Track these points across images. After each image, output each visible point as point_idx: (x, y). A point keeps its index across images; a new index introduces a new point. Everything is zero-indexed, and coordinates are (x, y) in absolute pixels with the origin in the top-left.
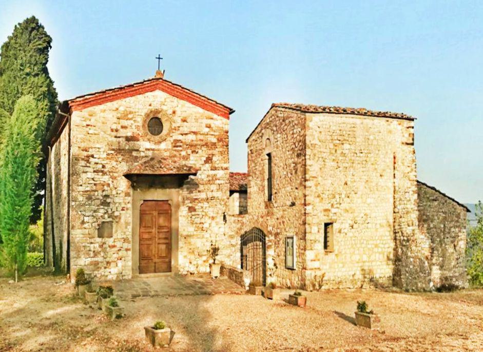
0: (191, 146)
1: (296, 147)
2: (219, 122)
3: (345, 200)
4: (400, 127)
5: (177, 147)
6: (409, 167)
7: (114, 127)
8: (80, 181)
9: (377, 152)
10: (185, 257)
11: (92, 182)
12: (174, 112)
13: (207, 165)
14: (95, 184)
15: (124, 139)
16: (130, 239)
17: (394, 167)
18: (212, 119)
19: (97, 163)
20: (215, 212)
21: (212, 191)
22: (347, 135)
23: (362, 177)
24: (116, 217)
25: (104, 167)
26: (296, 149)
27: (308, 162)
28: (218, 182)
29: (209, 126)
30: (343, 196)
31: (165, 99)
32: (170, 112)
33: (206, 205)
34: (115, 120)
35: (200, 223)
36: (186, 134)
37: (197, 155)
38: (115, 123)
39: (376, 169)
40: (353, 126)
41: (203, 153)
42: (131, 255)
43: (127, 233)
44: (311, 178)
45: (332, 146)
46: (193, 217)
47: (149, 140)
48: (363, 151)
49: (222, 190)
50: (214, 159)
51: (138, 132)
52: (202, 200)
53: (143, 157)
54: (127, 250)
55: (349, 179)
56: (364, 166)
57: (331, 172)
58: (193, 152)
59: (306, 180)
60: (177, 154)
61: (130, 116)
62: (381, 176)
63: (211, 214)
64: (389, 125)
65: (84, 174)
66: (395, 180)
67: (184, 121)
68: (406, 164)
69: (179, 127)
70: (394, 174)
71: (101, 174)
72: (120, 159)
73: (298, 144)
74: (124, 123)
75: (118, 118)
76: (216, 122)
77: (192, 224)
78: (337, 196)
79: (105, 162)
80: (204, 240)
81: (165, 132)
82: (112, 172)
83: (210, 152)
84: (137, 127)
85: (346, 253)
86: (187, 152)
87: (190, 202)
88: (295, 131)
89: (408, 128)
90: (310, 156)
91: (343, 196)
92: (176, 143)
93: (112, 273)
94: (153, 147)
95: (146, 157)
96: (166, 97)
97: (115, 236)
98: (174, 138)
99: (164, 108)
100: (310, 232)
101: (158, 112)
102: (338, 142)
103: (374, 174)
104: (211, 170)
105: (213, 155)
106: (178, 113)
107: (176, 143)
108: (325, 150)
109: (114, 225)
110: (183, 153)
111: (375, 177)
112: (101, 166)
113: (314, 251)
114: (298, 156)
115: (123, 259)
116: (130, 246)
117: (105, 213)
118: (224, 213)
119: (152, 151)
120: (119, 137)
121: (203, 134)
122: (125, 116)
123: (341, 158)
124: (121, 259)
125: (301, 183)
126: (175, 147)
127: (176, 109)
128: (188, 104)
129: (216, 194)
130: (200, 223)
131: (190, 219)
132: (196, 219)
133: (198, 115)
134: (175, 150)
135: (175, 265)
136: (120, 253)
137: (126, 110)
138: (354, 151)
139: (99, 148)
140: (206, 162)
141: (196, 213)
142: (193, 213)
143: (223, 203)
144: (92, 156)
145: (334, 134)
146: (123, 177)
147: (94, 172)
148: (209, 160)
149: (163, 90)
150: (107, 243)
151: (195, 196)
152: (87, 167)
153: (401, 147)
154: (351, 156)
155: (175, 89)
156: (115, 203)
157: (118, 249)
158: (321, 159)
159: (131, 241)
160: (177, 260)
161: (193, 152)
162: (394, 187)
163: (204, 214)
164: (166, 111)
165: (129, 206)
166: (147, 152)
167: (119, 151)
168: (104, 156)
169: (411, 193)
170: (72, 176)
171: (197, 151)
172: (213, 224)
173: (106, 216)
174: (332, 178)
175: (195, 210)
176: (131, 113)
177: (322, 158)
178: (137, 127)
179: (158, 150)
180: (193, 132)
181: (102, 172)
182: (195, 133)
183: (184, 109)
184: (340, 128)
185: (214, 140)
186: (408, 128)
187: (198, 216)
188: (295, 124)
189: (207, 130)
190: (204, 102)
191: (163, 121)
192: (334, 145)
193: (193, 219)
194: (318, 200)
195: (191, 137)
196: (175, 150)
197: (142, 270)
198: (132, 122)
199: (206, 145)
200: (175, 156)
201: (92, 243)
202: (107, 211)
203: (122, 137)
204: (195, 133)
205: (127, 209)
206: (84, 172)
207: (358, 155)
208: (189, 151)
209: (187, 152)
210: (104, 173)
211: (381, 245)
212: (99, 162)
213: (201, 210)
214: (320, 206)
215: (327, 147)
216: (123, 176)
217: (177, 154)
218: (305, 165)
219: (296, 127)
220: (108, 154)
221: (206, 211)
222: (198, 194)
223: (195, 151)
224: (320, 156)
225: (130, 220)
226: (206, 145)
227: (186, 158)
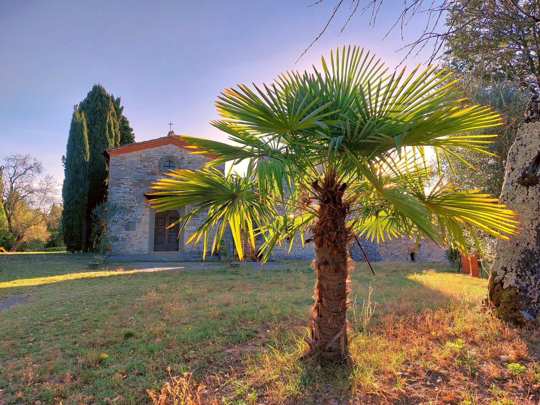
7: (139, 166)
11: (123, 199)
14: (124, 200)
15: (145, 174)
19: (126, 188)
24: (138, 219)
25: (130, 190)
31: (176, 150)
43: (146, 228)
54: (145, 238)
71: (128, 194)
82: (136, 193)
97: (137, 230)
99: (175, 155)
109: (137, 224)
116: (147, 236)
117: (131, 217)
136: (141, 240)
144: (123, 184)
149: (174, 144)
156: (138, 211)
164: (177, 157)
165: (148, 213)
167: (141, 181)
168: (131, 183)
173: (131, 218)
198: (151, 163)
201: (121, 233)
202: (132, 216)
205: (146, 215)
206: (116, 193)
210: (131, 194)
220: (134, 183)
225: (148, 221)
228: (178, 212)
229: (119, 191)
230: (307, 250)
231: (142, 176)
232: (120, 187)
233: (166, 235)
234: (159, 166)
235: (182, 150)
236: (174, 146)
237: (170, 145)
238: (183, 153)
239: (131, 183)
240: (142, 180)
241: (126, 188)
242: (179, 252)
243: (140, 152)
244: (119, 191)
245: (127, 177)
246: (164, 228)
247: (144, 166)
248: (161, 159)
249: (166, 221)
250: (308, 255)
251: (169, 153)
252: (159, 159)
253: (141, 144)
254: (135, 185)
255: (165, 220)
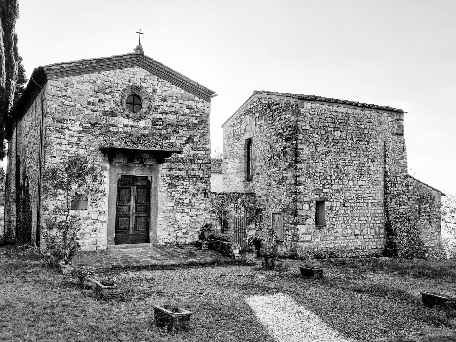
0: (172, 126)
1: (284, 132)
2: (200, 104)
3: (336, 181)
4: (390, 119)
5: (157, 125)
6: (399, 154)
7: (91, 100)
8: (54, 153)
9: (368, 140)
10: (164, 229)
11: (67, 154)
12: (154, 91)
13: (188, 145)
15: (101, 114)
16: (107, 212)
17: (385, 154)
18: (193, 100)
19: (72, 136)
20: (195, 189)
21: (193, 170)
22: (338, 123)
23: (354, 162)
25: (79, 140)
26: (285, 134)
27: (300, 146)
28: (199, 161)
29: (190, 107)
30: (334, 178)
31: (145, 76)
32: (150, 90)
33: (186, 182)
34: (93, 93)
35: (180, 199)
36: (167, 114)
37: (178, 135)
38: (92, 96)
39: (366, 155)
40: (344, 114)
41: (185, 133)
42: (106, 227)
43: (103, 206)
44: (302, 161)
45: (323, 133)
46: (174, 193)
47: (127, 116)
48: (354, 139)
49: (203, 170)
50: (196, 139)
51: (116, 107)
52: (182, 177)
53: (121, 133)
54: (102, 222)
55: (341, 163)
56: (355, 152)
57: (322, 156)
58: (173, 131)
59: (297, 162)
60: (157, 132)
61: (108, 90)
62: (372, 161)
63: (192, 191)
64: (380, 116)
65: (58, 146)
66: (386, 166)
67: (164, 100)
68: (396, 152)
69: (159, 106)
70: (385, 161)
71: (76, 147)
72: (97, 133)
73: (287, 129)
74: (102, 97)
75: (96, 92)
76: (197, 104)
77: (173, 199)
78: (329, 178)
79: (81, 135)
80: (184, 214)
81: (144, 110)
82: (88, 146)
83: (192, 133)
84: (115, 102)
85: (337, 228)
86: (167, 131)
87: (170, 179)
88: (283, 117)
89: (398, 120)
90: (301, 140)
91: (334, 178)
92: (156, 122)
93: (85, 244)
94: (132, 123)
95: (124, 133)
96: (146, 74)
98: (154, 116)
99: (144, 85)
100: (302, 209)
101: (138, 89)
102: (330, 129)
103: (365, 160)
104: (193, 150)
105: (195, 136)
106: (159, 91)
107: (156, 122)
108: (316, 136)
110: (163, 132)
111: (366, 163)
112: (76, 139)
113: (306, 226)
114: (287, 140)
115: (98, 230)
116: (106, 218)
118: (205, 190)
119: (130, 128)
120: (96, 111)
121: (184, 115)
122: (103, 90)
123: (332, 144)
124: (95, 231)
125: (290, 165)
126: (154, 125)
127: (157, 88)
128: (169, 84)
129: (196, 173)
130: (180, 199)
131: (169, 194)
132: (176, 195)
133: (179, 96)
134: (155, 129)
135: (153, 237)
136: (95, 226)
137: (104, 84)
138: (345, 137)
139: (74, 120)
140: (187, 142)
141: (177, 189)
142: (173, 189)
143: (204, 181)
144: (68, 128)
145: (325, 121)
146: (100, 152)
147: (69, 144)
148: (190, 140)
149: (143, 67)
150: (81, 215)
151: (176, 173)
152: (62, 139)
153: (391, 136)
154: (342, 142)
155: (156, 68)
157: (93, 221)
158: (312, 143)
159: (107, 214)
160: (155, 233)
161: (173, 131)
162: (386, 172)
163: (184, 190)
166: (126, 128)
168: (81, 128)
169: (402, 177)
170: (45, 147)
171: (177, 130)
172: (194, 200)
174: (323, 162)
175: (175, 187)
176: (109, 87)
177: (314, 142)
178: (115, 102)
179: (137, 127)
180: (173, 112)
181: (78, 144)
182: (175, 113)
183: (165, 88)
184: (331, 116)
185: (196, 122)
186: (398, 120)
187: (178, 192)
188: (283, 110)
189: (188, 111)
190: (186, 83)
191: (143, 98)
192: (325, 131)
193: (173, 195)
194: (309, 180)
195: (171, 117)
196: (155, 129)
197: (117, 241)
199: (187, 125)
200: (155, 134)
203: (100, 111)
204: (175, 113)
206: (58, 144)
207: (350, 142)
208: (170, 131)
209: (167, 131)
210: (79, 146)
211: (372, 222)
212: (75, 135)
213: (182, 187)
214: (311, 185)
215: (319, 133)
216: (100, 150)
217: (157, 132)
218: (297, 149)
219: (284, 113)
221: (187, 187)
222: (179, 172)
223: (175, 131)
224: (311, 141)
226: (187, 125)
227: (166, 137)
228: (149, 178)
229: (63, 141)
230: (340, 240)
231: (96, 116)
232: (62, 133)
233: (131, 217)
234: (122, 102)
235: (153, 78)
236: (143, 70)
237: (137, 69)
238: (155, 83)
239: (81, 128)
240: (96, 124)
241: (72, 136)
242: (150, 245)
243: (93, 76)
244: (63, 141)
245: (73, 118)
246: (129, 204)
247: (100, 101)
248: (125, 90)
249: (132, 194)
250: (342, 247)
251: (135, 82)
252: (121, 89)
253: (96, 63)
254: (86, 131)
255: (130, 191)
